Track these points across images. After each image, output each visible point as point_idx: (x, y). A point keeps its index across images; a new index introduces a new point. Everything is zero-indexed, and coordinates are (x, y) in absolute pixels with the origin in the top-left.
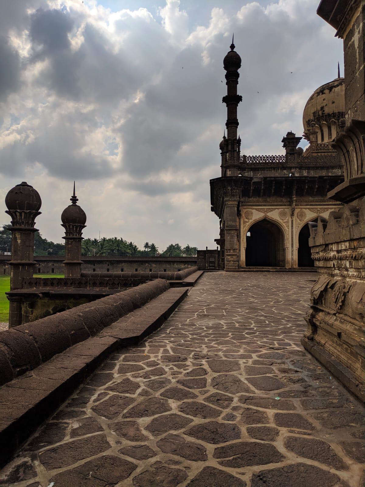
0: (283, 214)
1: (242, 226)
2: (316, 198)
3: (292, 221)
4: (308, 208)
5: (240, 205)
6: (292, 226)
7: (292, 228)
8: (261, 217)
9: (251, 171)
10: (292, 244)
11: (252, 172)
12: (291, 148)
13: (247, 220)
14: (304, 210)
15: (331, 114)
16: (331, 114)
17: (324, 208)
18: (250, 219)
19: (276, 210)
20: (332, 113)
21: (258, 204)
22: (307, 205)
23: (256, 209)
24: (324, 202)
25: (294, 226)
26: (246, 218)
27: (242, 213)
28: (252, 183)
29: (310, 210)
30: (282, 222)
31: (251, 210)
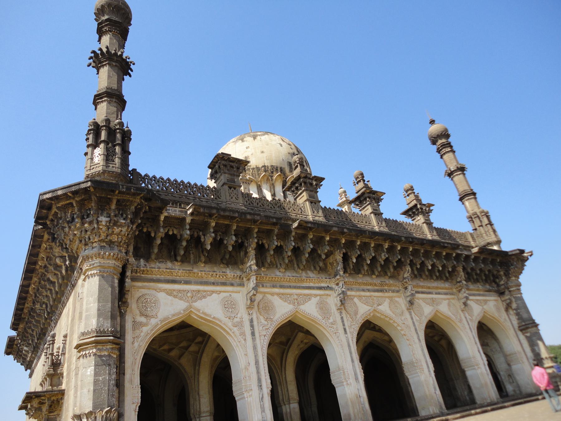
0: (229, 306)
3: (251, 321)
4: (278, 294)
5: (128, 273)
6: (253, 334)
7: (254, 339)
10: (259, 380)
12: (230, 176)
13: (143, 319)
14: (269, 296)
17: (305, 295)
18: (152, 317)
19: (214, 295)
20: (263, 166)
21: (170, 278)
23: (164, 290)
25: (257, 334)
26: (142, 314)
27: (129, 301)
28: (162, 218)
31: (154, 292)
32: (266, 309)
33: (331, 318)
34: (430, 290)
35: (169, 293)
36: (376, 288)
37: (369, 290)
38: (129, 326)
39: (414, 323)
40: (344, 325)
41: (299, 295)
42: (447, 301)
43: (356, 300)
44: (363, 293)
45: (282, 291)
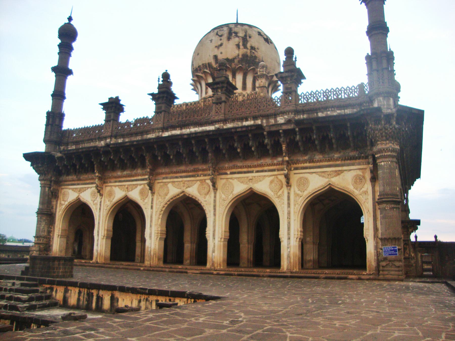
0: (93, 195)
1: (58, 210)
2: (125, 173)
3: (101, 202)
6: (100, 209)
13: (63, 202)
14: (113, 187)
17: (134, 185)
19: (89, 189)
22: (116, 182)
32: (111, 194)
35: (73, 189)
36: (190, 174)
37: (181, 177)
39: (215, 201)
40: (152, 203)
41: (128, 185)
42: (272, 178)
43: (170, 185)
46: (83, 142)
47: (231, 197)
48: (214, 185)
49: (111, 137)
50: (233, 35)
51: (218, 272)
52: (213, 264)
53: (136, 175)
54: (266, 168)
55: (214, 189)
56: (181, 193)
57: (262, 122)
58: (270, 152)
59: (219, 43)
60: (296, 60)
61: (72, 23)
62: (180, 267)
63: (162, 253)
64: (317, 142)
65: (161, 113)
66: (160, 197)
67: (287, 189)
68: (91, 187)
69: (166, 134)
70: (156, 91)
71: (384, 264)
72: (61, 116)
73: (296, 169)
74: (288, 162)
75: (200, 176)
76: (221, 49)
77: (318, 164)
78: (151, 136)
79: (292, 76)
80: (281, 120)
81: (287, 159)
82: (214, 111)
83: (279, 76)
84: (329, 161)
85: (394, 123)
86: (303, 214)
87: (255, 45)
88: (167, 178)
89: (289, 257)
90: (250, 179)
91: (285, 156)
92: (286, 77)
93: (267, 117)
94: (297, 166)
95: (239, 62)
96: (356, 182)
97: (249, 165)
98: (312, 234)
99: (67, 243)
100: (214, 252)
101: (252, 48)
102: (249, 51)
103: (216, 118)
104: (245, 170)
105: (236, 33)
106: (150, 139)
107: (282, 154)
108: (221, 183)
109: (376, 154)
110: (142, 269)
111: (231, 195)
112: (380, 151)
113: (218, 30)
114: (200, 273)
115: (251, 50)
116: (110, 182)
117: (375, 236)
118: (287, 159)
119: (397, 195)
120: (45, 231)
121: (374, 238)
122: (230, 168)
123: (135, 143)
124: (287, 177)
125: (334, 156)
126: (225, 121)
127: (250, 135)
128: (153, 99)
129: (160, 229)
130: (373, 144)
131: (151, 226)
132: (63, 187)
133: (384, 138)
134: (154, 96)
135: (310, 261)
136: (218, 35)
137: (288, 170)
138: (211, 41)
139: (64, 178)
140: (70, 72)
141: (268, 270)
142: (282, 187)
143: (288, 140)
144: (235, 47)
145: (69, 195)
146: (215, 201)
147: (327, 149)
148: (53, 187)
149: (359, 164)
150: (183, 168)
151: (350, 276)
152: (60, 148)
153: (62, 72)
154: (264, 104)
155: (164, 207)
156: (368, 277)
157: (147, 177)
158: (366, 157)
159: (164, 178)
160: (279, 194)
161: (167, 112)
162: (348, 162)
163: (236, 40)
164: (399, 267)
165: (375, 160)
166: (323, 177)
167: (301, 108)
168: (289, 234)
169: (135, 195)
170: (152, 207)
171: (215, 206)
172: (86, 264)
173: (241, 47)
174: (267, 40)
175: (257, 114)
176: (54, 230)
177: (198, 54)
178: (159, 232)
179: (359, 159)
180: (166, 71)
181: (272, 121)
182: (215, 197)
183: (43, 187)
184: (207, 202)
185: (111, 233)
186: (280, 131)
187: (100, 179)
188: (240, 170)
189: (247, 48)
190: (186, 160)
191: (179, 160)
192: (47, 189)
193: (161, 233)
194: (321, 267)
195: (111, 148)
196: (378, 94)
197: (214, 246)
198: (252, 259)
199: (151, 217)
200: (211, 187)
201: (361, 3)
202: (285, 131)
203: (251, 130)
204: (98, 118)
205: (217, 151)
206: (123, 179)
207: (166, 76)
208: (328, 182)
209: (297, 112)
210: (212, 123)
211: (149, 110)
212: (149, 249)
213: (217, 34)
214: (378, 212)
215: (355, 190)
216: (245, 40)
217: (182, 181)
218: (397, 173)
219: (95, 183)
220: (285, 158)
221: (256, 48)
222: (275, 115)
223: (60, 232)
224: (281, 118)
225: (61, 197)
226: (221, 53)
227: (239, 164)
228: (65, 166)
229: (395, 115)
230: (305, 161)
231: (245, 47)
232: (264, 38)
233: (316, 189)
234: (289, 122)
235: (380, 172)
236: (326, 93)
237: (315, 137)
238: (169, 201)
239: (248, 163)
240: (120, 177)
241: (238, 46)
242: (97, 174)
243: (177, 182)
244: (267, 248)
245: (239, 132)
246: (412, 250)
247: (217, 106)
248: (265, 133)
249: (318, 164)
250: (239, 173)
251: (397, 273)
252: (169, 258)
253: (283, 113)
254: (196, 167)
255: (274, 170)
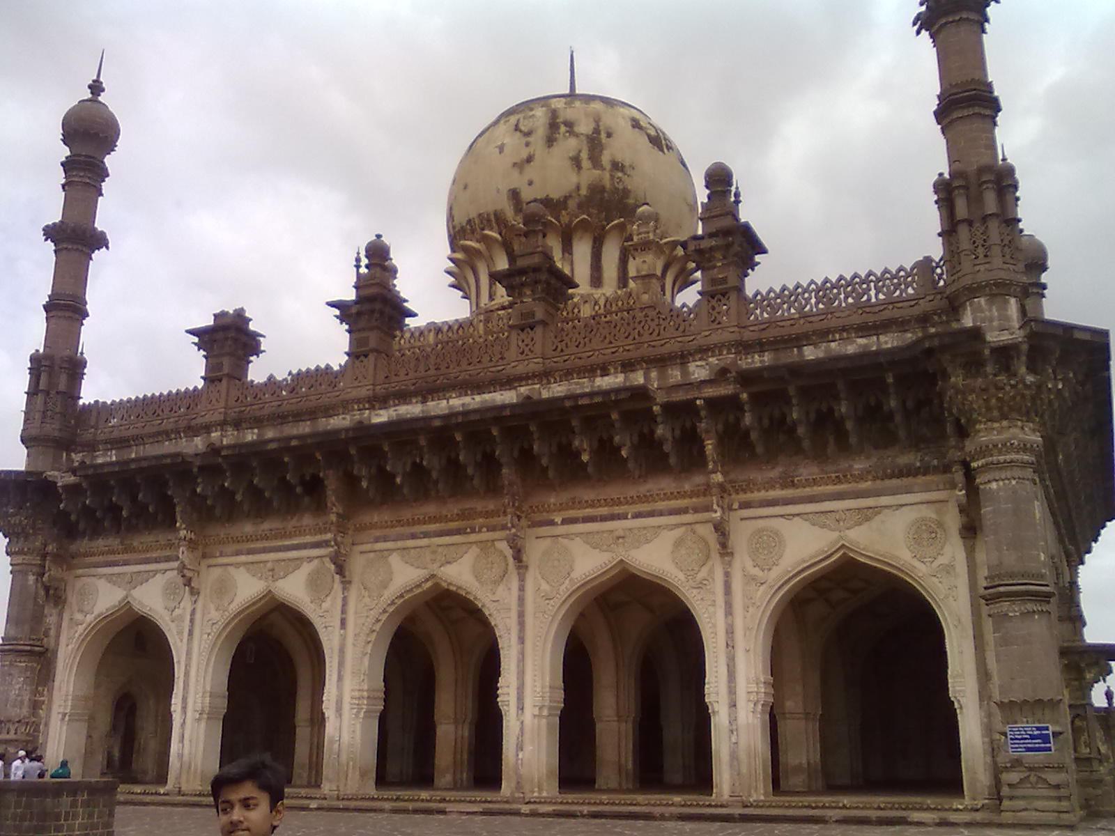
0: (170, 591)
1: (63, 640)
2: (266, 526)
3: (193, 612)
4: (245, 564)
6: (191, 633)
8: (115, 606)
9: (111, 449)
11: (114, 452)
13: (79, 616)
15: (464, 224)
16: (464, 224)
17: (289, 560)
22: (238, 553)
24: (290, 536)
26: (81, 611)
29: (248, 570)
30: (167, 618)
31: (94, 579)
32: (223, 589)
33: (329, 598)
34: (617, 510)
35: (110, 578)
36: (453, 525)
37: (426, 535)
38: (65, 624)
39: (521, 600)
42: (678, 533)
43: (395, 560)
44: (411, 543)
45: (251, 558)
46: (139, 439)
47: (566, 587)
48: (518, 555)
49: (222, 424)
50: (563, 129)
51: (532, 807)
52: (519, 786)
53: (300, 532)
54: (661, 505)
55: (519, 568)
56: (427, 580)
57: (646, 377)
58: (672, 460)
59: (524, 155)
60: (737, 202)
61: (102, 98)
62: (424, 795)
63: (371, 759)
64: (801, 431)
65: (366, 356)
66: (367, 594)
67: (723, 563)
68: (166, 570)
69: (381, 417)
70: (351, 295)
71: (1013, 777)
72: (76, 368)
73: (746, 505)
74: (722, 488)
75: (480, 531)
76: (531, 172)
77: (808, 491)
78: (339, 422)
79: (728, 246)
80: (699, 371)
81: (718, 478)
82: (513, 348)
83: (691, 247)
84: (838, 481)
85: (1023, 370)
86: (771, 633)
87: (624, 157)
88: (385, 539)
89: (734, 756)
90: (618, 538)
91: (715, 472)
92: (711, 249)
93: (661, 362)
94: (749, 496)
95: (580, 206)
96: (917, 541)
97: (615, 497)
98: (799, 688)
99: (89, 737)
100: (520, 747)
101: (617, 166)
102: (607, 175)
103: (521, 369)
104: (604, 511)
105: (569, 125)
106: (336, 432)
107: (705, 464)
108: (536, 549)
109: (973, 459)
110: (313, 805)
111: (567, 582)
112: (984, 451)
113: (521, 116)
114: (483, 813)
115: (611, 171)
116: (221, 555)
117: (984, 694)
118: (718, 478)
119: (1042, 576)
120: (22, 702)
121: (981, 699)
122: (562, 508)
123: (294, 443)
124: (721, 529)
125: (851, 466)
126: (545, 376)
127: (615, 416)
128: (342, 319)
129: (366, 687)
130: (963, 432)
131: (340, 678)
132: (80, 572)
133: (996, 413)
134: (345, 311)
135: (798, 769)
136: (521, 131)
137: (722, 508)
138: (501, 149)
139: (83, 545)
140: (100, 241)
141: (677, 799)
142: (708, 557)
143: (720, 427)
144: (568, 163)
145: (101, 594)
146: (521, 600)
147: (831, 448)
148: (53, 571)
149: (927, 489)
150: (431, 509)
151: (916, 816)
152: (70, 460)
153: (76, 240)
154: (653, 325)
155: (378, 621)
156: (966, 817)
157: (329, 536)
158: (946, 469)
159: (377, 540)
160: (700, 576)
161: (383, 352)
162: (895, 482)
163: (569, 145)
164: (1058, 787)
165: (970, 475)
166: (823, 526)
167: (755, 336)
168: (732, 691)
169: (294, 588)
170: (343, 623)
171: (521, 615)
172: (148, 799)
173: (586, 164)
174: (658, 141)
175: (635, 354)
176: (50, 700)
177: (465, 187)
178: (365, 694)
179: (924, 475)
180: (379, 236)
181: (675, 375)
182: (522, 589)
183: (17, 572)
184: (499, 604)
185: (223, 704)
186: (698, 402)
187: (192, 545)
188: (589, 512)
189: (604, 169)
190: (440, 486)
191: (422, 484)
192: (31, 578)
193: (368, 697)
194: (832, 788)
195: (225, 457)
196: (973, 291)
197: (522, 730)
198: (630, 766)
199: (342, 651)
200: (511, 560)
201: (918, 33)
202: (712, 403)
203: (617, 402)
204: (189, 370)
205: (526, 460)
206: (259, 545)
207: (378, 255)
208: (837, 541)
209: (745, 347)
210: (509, 382)
211: (329, 345)
212: (336, 746)
213: (517, 128)
214: (988, 625)
215: (916, 563)
216: (595, 143)
217: (428, 546)
218: (1038, 510)
219: (177, 558)
220: (713, 476)
221: (627, 164)
222: (683, 358)
223: (70, 703)
224: (699, 363)
225: (72, 598)
226: (530, 183)
227: (587, 494)
228: (88, 512)
229: (1025, 347)
230: (770, 485)
231: (595, 161)
232: (649, 136)
233: (804, 561)
234: (722, 374)
235: (986, 510)
236: (825, 290)
237: (795, 416)
238: (393, 603)
239: (613, 491)
240: (249, 539)
241: (576, 162)
242: (183, 533)
243: (415, 548)
244: (674, 732)
245: (582, 406)
246: (1099, 734)
247: (523, 336)
248: (656, 409)
249: (808, 491)
250: (587, 520)
251: (1053, 804)
252: (393, 769)
253: (704, 351)
254: (468, 504)
255: (684, 511)
